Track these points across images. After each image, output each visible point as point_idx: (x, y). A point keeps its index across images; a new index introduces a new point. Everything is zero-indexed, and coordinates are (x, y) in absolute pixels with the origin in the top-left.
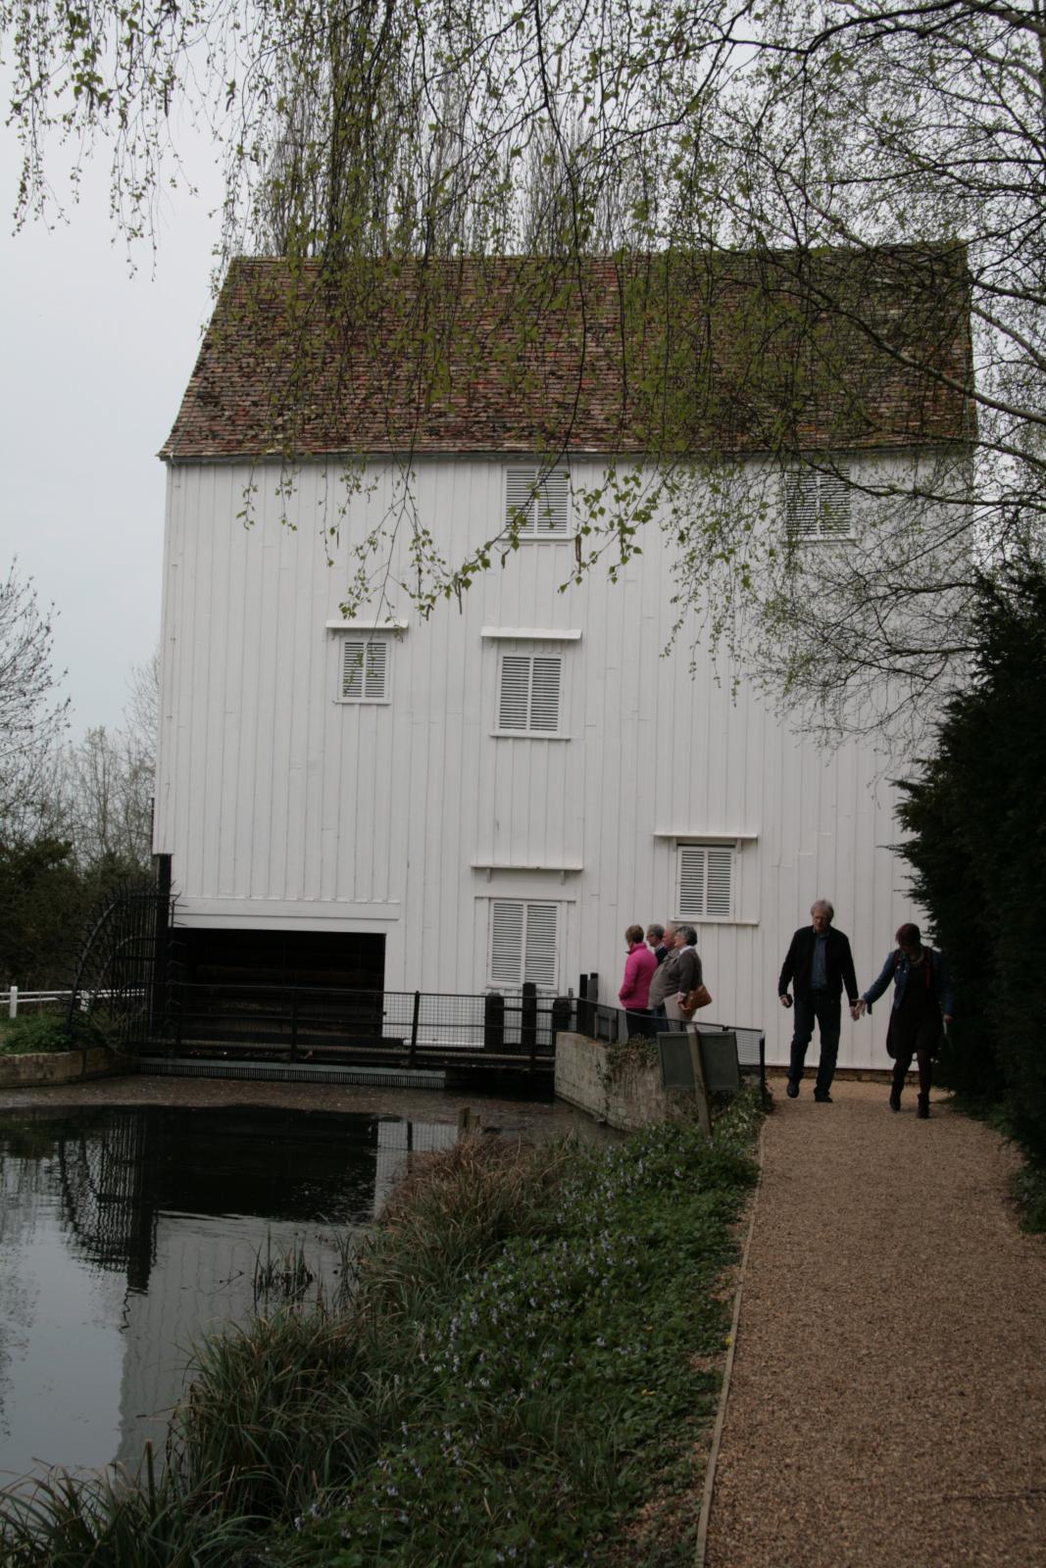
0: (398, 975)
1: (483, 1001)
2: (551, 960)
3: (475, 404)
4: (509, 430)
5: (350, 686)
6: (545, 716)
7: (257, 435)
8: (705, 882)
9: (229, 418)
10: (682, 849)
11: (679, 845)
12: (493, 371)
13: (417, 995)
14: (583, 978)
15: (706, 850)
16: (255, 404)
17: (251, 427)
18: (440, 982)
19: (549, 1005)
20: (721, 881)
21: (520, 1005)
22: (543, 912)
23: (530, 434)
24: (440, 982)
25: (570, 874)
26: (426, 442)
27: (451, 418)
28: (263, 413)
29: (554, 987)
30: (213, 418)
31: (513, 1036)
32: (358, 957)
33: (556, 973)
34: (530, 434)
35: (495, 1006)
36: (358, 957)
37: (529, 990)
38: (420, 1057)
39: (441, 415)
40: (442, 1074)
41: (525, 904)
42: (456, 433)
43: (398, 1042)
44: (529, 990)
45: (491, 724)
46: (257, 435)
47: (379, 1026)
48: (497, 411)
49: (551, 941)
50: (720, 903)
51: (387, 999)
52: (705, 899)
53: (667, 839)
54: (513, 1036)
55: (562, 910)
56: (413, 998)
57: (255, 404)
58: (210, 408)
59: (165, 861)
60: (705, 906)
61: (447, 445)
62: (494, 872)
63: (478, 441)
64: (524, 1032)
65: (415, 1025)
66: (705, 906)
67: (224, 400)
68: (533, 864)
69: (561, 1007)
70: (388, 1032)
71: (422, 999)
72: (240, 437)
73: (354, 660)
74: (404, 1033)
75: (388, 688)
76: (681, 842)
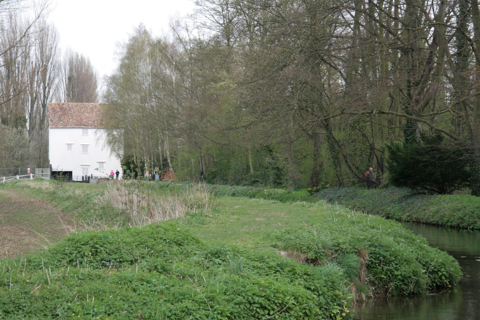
5: (68, 149)
6: (87, 151)
18: (77, 176)
22: (87, 169)
25: (89, 165)
26: (74, 126)
31: (85, 179)
32: (70, 173)
35: (83, 177)
36: (70, 173)
37: (86, 176)
42: (77, 125)
44: (86, 176)
54: (85, 179)
59: (51, 165)
61: (76, 127)
62: (82, 165)
69: (89, 177)
70: (73, 180)
73: (68, 146)
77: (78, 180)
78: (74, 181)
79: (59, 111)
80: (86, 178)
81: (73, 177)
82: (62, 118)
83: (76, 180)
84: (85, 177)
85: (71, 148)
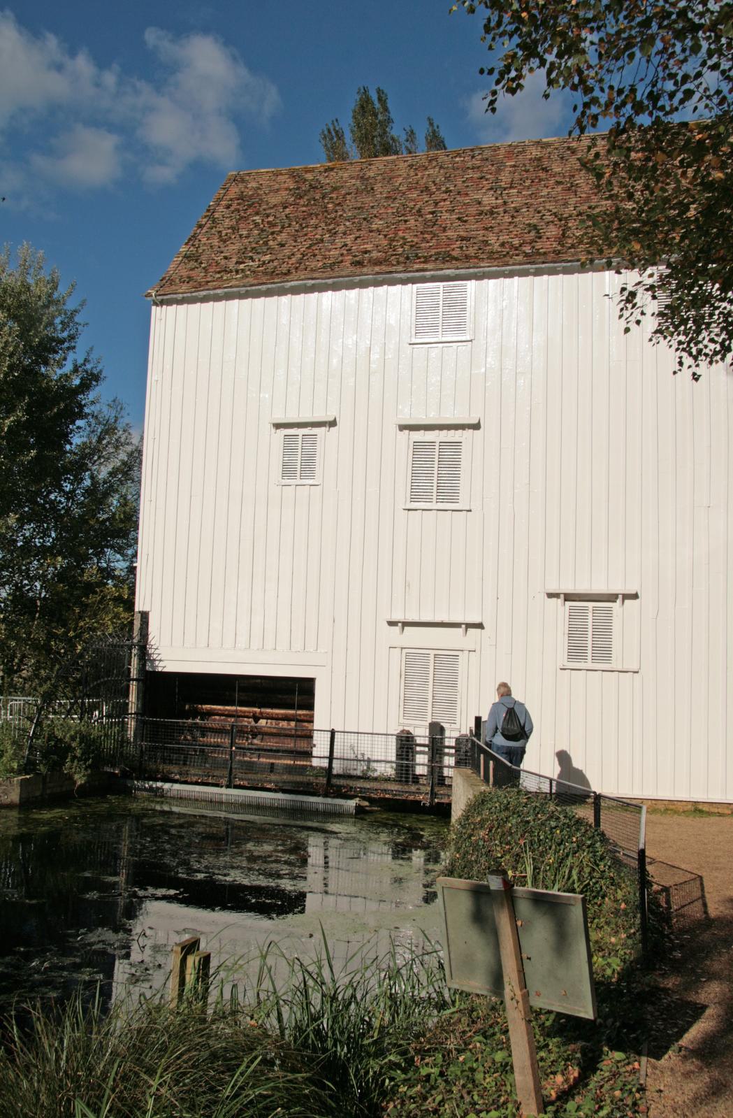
0: (324, 715)
2: (453, 702)
3: (394, 243)
4: (419, 258)
5: (288, 471)
6: (448, 492)
7: (222, 277)
8: (590, 633)
9: (204, 268)
10: (568, 604)
11: (565, 600)
12: (412, 223)
13: (333, 733)
14: (478, 720)
16: (226, 258)
17: (219, 272)
18: (359, 722)
20: (603, 630)
21: (427, 742)
22: (447, 659)
23: (437, 259)
24: (359, 722)
27: (375, 254)
28: (231, 265)
29: (457, 726)
30: (192, 269)
31: (420, 770)
33: (458, 713)
34: (437, 259)
37: (437, 730)
39: (366, 252)
40: (352, 803)
41: (432, 653)
42: (378, 262)
44: (437, 730)
45: (403, 500)
46: (222, 277)
48: (412, 246)
49: (454, 685)
50: (603, 652)
51: (316, 734)
52: (590, 648)
53: (556, 595)
55: (463, 657)
56: (329, 735)
57: (226, 258)
58: (192, 263)
59: (145, 616)
60: (590, 655)
63: (393, 265)
64: (428, 766)
65: (331, 758)
66: (590, 655)
67: (203, 258)
68: (438, 619)
71: (337, 736)
72: (209, 279)
74: (325, 763)
75: (318, 471)
76: (568, 597)
80: (436, 748)
82: (282, 237)
84: (421, 734)
85: (308, 467)
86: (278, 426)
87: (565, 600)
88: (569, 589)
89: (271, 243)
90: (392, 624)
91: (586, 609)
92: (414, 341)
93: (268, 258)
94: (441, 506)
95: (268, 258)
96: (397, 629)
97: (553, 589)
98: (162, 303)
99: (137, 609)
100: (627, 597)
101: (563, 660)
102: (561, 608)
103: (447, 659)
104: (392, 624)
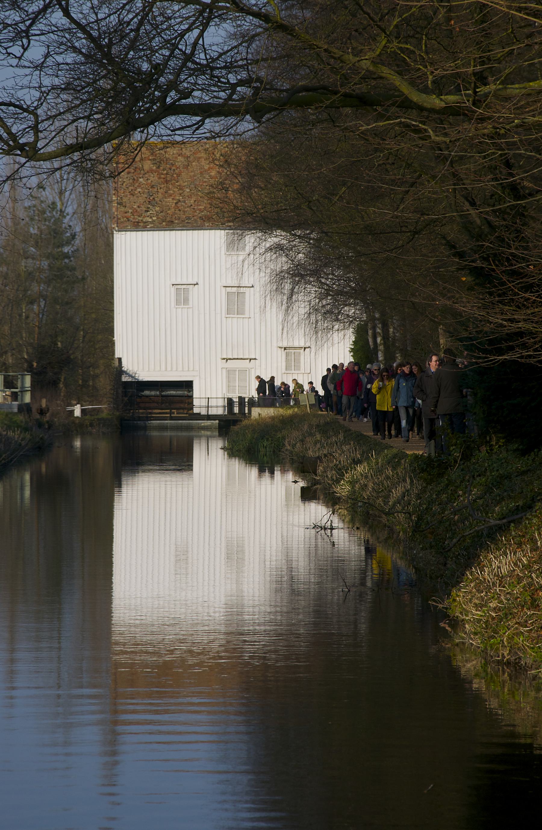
0: (197, 392)
1: (226, 399)
5: (178, 302)
6: (240, 311)
11: (285, 349)
15: (293, 351)
19: (246, 400)
31: (236, 410)
35: (230, 402)
38: (209, 417)
40: (217, 421)
43: (199, 414)
47: (192, 409)
53: (282, 348)
54: (236, 410)
59: (120, 359)
76: (285, 349)
77: (213, 412)
78: (199, 417)
79: (151, 171)
81: (196, 402)
83: (204, 412)
85: (186, 301)
86: (173, 285)
87: (285, 349)
88: (285, 345)
89: (156, 199)
90: (224, 359)
91: (291, 352)
92: (227, 253)
93: (157, 209)
94: (238, 316)
95: (157, 209)
96: (225, 361)
97: (281, 345)
98: (119, 231)
99: (116, 357)
100: (305, 348)
101: (284, 370)
102: (283, 352)
103: (243, 372)
104: (224, 359)
